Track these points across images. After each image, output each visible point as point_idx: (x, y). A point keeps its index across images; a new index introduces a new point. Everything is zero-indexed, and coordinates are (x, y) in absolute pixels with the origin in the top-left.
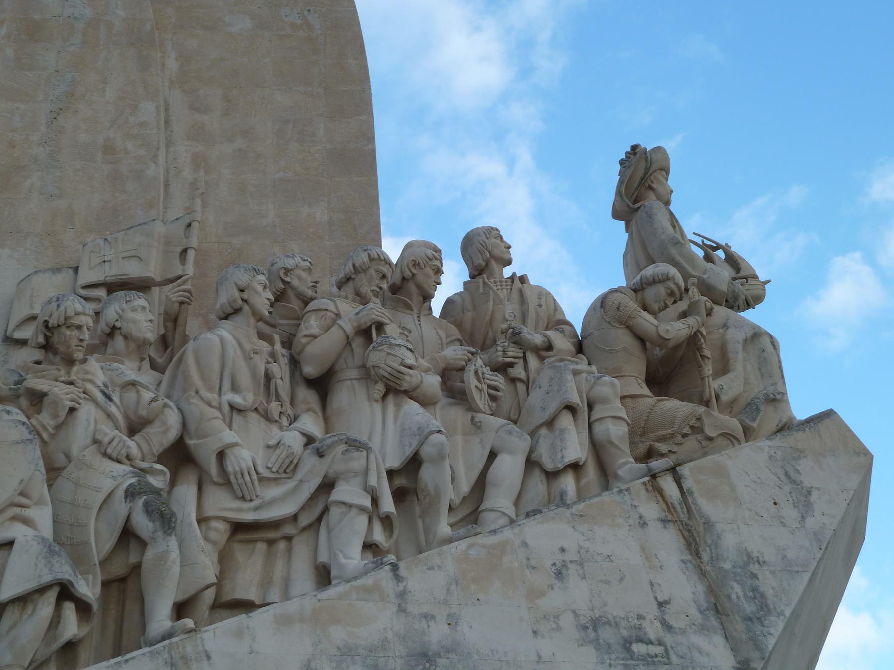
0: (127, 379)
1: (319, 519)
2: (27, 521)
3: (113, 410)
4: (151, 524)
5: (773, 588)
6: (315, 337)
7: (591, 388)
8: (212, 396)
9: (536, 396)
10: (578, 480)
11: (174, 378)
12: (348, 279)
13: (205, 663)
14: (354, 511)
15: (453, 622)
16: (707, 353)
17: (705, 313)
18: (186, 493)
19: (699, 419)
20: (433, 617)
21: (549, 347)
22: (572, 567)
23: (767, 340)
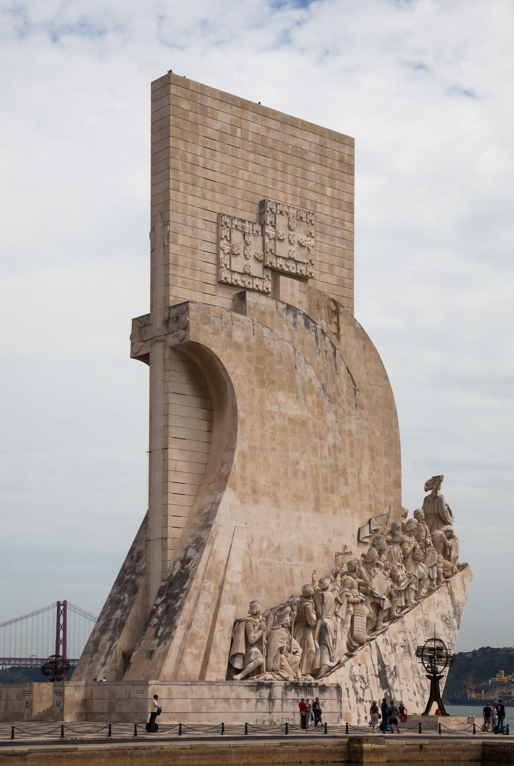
1: (405, 590)
4: (396, 595)
6: (407, 549)
12: (409, 531)
19: (452, 568)
21: (430, 545)
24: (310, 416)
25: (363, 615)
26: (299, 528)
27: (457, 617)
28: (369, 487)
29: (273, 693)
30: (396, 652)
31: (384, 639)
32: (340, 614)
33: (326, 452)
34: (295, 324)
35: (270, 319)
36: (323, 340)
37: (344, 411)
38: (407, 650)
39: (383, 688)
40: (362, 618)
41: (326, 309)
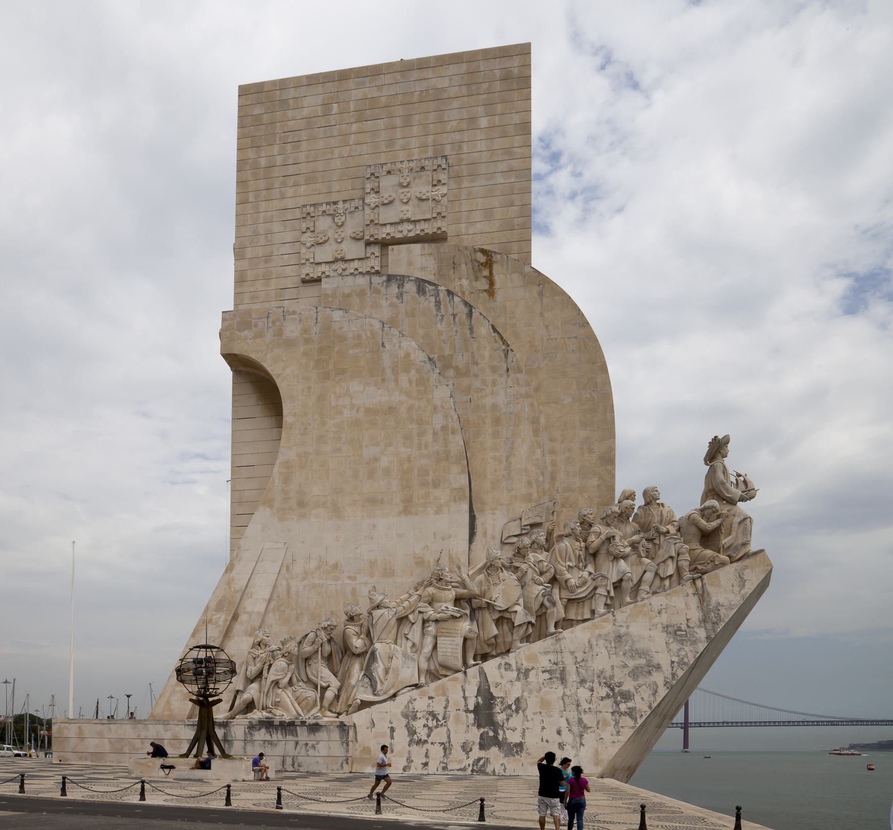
2: (518, 604)
3: (537, 569)
5: (724, 614)
6: (593, 542)
7: (680, 549)
9: (661, 552)
11: (552, 555)
12: (604, 518)
13: (564, 640)
14: (602, 596)
15: (628, 627)
16: (723, 532)
17: (724, 517)
18: (556, 591)
20: (622, 626)
21: (668, 532)
22: (664, 611)
24: (403, 398)
25: (454, 635)
26: (372, 538)
27: (709, 626)
29: (231, 733)
30: (528, 680)
31: (503, 663)
33: (429, 438)
34: (400, 296)
35: (358, 300)
36: (450, 302)
37: (484, 382)
38: (558, 675)
39: (479, 726)
40: (451, 639)
41: (470, 266)
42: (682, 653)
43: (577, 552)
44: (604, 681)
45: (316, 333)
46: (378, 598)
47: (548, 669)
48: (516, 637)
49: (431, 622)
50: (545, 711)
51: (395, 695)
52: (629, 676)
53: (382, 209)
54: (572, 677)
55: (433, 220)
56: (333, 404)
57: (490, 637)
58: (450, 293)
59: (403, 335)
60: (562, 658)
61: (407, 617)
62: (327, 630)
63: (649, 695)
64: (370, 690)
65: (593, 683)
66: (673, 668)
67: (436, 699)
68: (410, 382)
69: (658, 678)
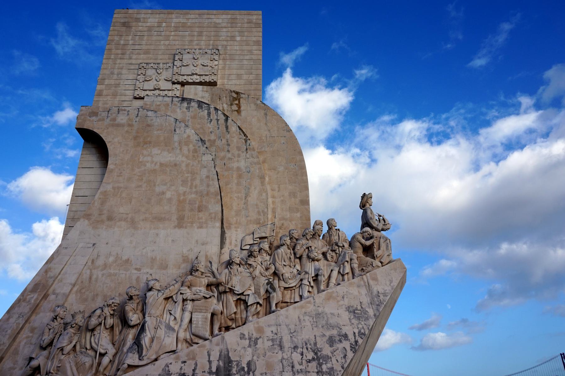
0: (266, 260)
1: (300, 286)
2: (250, 290)
3: (263, 266)
8: (279, 263)
9: (340, 258)
10: (348, 276)
12: (305, 235)
13: (282, 317)
16: (375, 246)
18: (276, 281)
19: (372, 262)
21: (344, 246)
23: (388, 241)
24: (184, 159)
25: (204, 311)
26: (155, 243)
27: (374, 307)
28: (257, 205)
30: (257, 346)
32: (172, 312)
34: (188, 108)
36: (216, 113)
38: (278, 343)
40: (202, 314)
41: (228, 98)
42: (360, 326)
43: (289, 255)
44: (310, 347)
45: (136, 121)
46: (151, 283)
47: (271, 338)
48: (249, 314)
49: (188, 301)
50: (269, 372)
51: (156, 360)
52: (327, 343)
53: (183, 68)
54: (287, 344)
55: (210, 75)
56: (141, 160)
57: (231, 313)
58: (216, 109)
59: (187, 127)
60: (280, 329)
61: (172, 297)
62: (112, 307)
63: (342, 358)
64: (136, 356)
65: (302, 348)
66: (355, 337)
67: (188, 362)
68: (189, 150)
69: (346, 344)
